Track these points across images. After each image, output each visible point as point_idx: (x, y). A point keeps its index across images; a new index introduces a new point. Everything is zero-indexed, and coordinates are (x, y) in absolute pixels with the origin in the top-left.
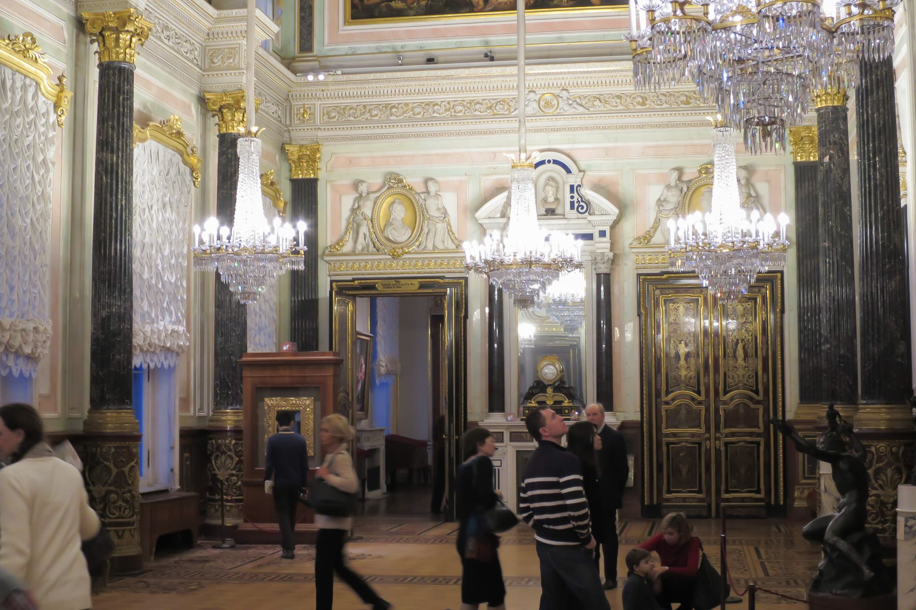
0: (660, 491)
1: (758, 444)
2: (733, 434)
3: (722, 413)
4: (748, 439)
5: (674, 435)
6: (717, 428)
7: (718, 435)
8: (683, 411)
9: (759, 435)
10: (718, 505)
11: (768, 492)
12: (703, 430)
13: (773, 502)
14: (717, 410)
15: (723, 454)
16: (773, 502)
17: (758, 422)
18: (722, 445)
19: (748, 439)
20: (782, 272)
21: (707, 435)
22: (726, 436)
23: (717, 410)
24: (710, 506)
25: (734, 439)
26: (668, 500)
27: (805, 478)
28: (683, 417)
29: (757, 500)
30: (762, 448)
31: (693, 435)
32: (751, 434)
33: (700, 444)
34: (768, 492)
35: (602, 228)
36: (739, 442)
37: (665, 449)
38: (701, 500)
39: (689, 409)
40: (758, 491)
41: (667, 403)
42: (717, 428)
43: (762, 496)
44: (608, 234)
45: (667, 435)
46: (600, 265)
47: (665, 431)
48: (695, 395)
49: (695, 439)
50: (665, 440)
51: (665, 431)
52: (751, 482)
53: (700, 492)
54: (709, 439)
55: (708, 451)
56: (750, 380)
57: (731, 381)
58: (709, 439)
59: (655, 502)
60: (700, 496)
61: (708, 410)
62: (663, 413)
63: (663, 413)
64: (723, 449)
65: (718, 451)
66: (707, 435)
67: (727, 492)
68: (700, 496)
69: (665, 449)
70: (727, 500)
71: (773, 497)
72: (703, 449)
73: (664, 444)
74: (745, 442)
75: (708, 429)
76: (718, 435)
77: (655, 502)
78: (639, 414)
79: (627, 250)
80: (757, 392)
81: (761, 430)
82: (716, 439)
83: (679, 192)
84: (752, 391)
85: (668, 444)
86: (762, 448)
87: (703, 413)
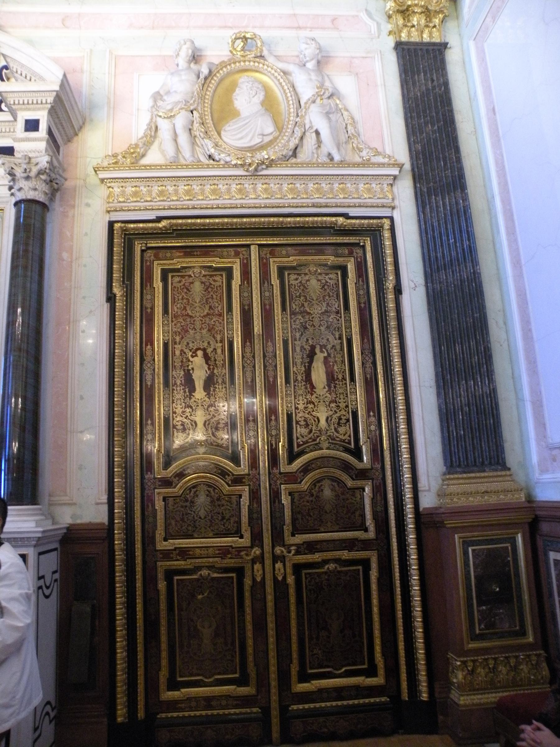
0: (152, 687)
1: (366, 563)
2: (311, 547)
3: (285, 500)
4: (345, 555)
5: (183, 553)
6: (278, 537)
7: (278, 550)
8: (202, 499)
9: (366, 545)
10: (283, 709)
11: (392, 671)
12: (245, 541)
13: (405, 696)
14: (275, 496)
15: (292, 591)
16: (405, 696)
17: (363, 516)
18: (289, 570)
19: (345, 555)
20: (391, 219)
21: (256, 551)
22: (298, 553)
23: (275, 496)
24: (266, 711)
25: (317, 557)
26: (173, 705)
27: (475, 638)
28: (202, 513)
29: (371, 691)
30: (374, 574)
31: (224, 552)
32: (350, 545)
33: (240, 571)
34: (392, 671)
35: (31, 115)
36: (326, 562)
37: (162, 585)
38: (245, 701)
39: (217, 499)
40: (372, 672)
41: (167, 483)
42: (278, 537)
43: (378, 680)
44: (43, 126)
45: (167, 555)
46: (22, 183)
47: (162, 545)
48: (229, 465)
49: (229, 562)
50: (162, 565)
51: (162, 545)
52: (352, 653)
53: (242, 681)
54: (261, 559)
55: (259, 587)
56: (342, 430)
57: (304, 431)
58: (261, 559)
59: (141, 714)
60: (243, 690)
61: (255, 495)
62: (159, 505)
63: (159, 505)
64: (291, 580)
65: (280, 586)
66: (256, 551)
67: (304, 678)
68: (243, 690)
69: (162, 585)
70: (305, 697)
71: (404, 685)
72: (248, 582)
73: (160, 575)
74: (337, 561)
75: (257, 538)
76: (278, 550)
77: (141, 714)
78: (105, 508)
79: (93, 179)
80: (357, 453)
81: (371, 534)
82: (275, 559)
83: (194, 77)
84: (347, 450)
85: (170, 574)
86: (374, 574)
87: (245, 501)
